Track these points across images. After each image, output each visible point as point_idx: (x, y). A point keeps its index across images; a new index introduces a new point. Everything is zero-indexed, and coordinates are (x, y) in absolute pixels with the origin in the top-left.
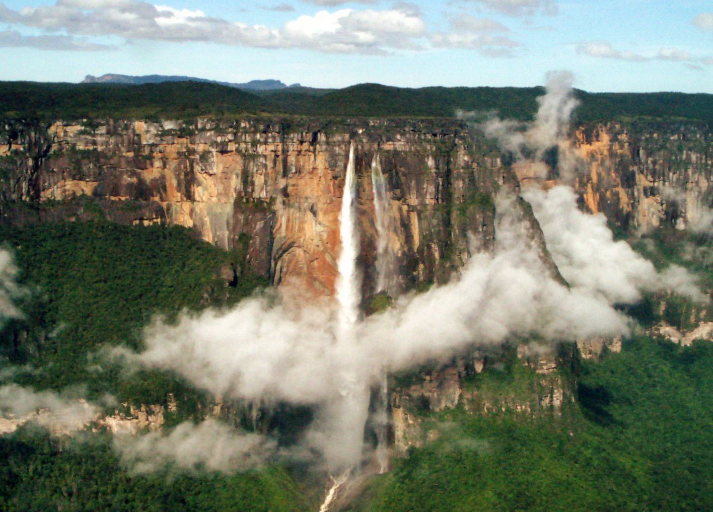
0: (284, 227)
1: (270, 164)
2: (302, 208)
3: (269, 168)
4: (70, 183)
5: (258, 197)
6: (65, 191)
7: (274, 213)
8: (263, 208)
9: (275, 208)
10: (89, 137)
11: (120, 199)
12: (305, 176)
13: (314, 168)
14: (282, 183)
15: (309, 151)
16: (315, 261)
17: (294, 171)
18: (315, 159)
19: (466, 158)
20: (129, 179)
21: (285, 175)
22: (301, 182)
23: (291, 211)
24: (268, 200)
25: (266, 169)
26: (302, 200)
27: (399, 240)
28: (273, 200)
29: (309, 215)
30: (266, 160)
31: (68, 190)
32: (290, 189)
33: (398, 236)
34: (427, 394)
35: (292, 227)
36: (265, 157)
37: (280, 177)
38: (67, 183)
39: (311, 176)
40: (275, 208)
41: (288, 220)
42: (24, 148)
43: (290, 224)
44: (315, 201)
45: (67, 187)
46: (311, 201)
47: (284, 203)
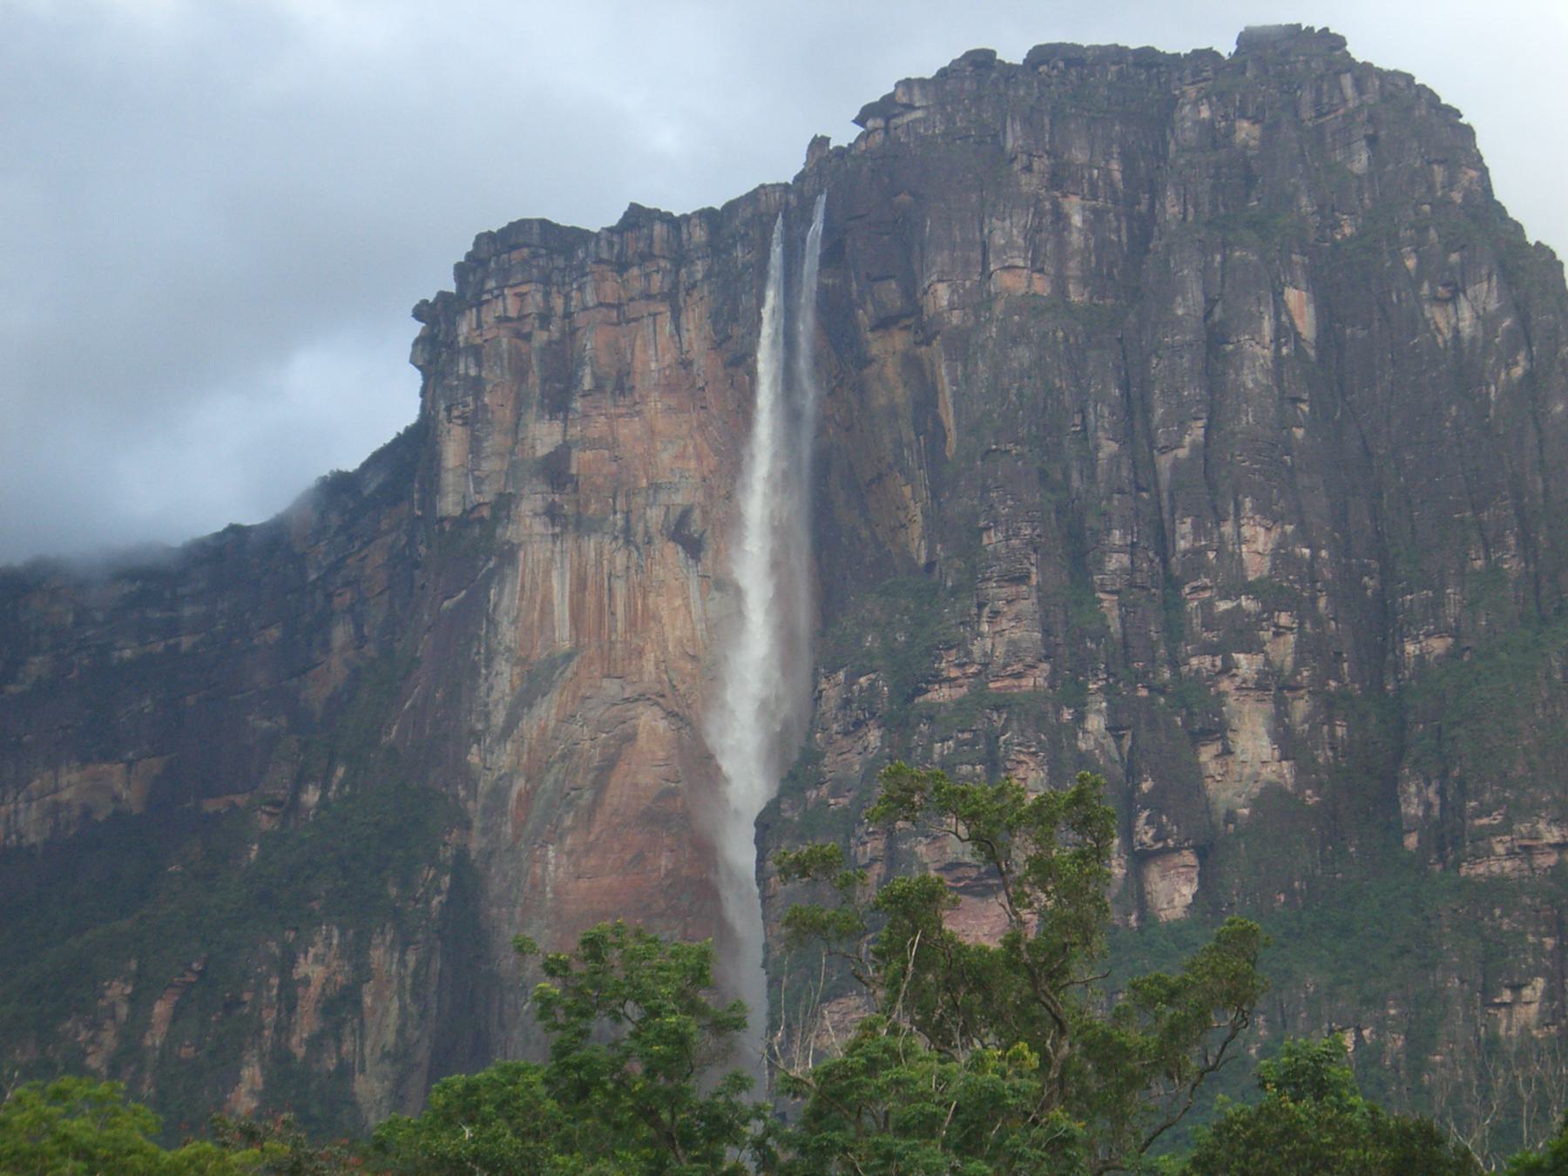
0: (561, 610)
1: (494, 374)
2: (640, 528)
3: (489, 388)
4: (75, 777)
5: (457, 512)
6: (57, 806)
7: (509, 555)
8: (476, 549)
9: (510, 533)
10: (156, 615)
11: (233, 806)
14: (544, 436)
15: (648, 296)
17: (587, 383)
18: (678, 328)
19: (1205, 113)
20: (266, 724)
21: (557, 405)
22: (629, 430)
23: (590, 545)
24: (486, 513)
25: (477, 398)
26: (640, 500)
28: (504, 505)
29: (673, 554)
30: (479, 365)
31: (68, 804)
32: (579, 461)
33: (910, 481)
36: (476, 351)
37: (530, 416)
38: (63, 781)
39: (673, 402)
40: (510, 533)
41: (580, 584)
43: (590, 600)
45: (66, 795)
46: (678, 499)
47: (552, 513)
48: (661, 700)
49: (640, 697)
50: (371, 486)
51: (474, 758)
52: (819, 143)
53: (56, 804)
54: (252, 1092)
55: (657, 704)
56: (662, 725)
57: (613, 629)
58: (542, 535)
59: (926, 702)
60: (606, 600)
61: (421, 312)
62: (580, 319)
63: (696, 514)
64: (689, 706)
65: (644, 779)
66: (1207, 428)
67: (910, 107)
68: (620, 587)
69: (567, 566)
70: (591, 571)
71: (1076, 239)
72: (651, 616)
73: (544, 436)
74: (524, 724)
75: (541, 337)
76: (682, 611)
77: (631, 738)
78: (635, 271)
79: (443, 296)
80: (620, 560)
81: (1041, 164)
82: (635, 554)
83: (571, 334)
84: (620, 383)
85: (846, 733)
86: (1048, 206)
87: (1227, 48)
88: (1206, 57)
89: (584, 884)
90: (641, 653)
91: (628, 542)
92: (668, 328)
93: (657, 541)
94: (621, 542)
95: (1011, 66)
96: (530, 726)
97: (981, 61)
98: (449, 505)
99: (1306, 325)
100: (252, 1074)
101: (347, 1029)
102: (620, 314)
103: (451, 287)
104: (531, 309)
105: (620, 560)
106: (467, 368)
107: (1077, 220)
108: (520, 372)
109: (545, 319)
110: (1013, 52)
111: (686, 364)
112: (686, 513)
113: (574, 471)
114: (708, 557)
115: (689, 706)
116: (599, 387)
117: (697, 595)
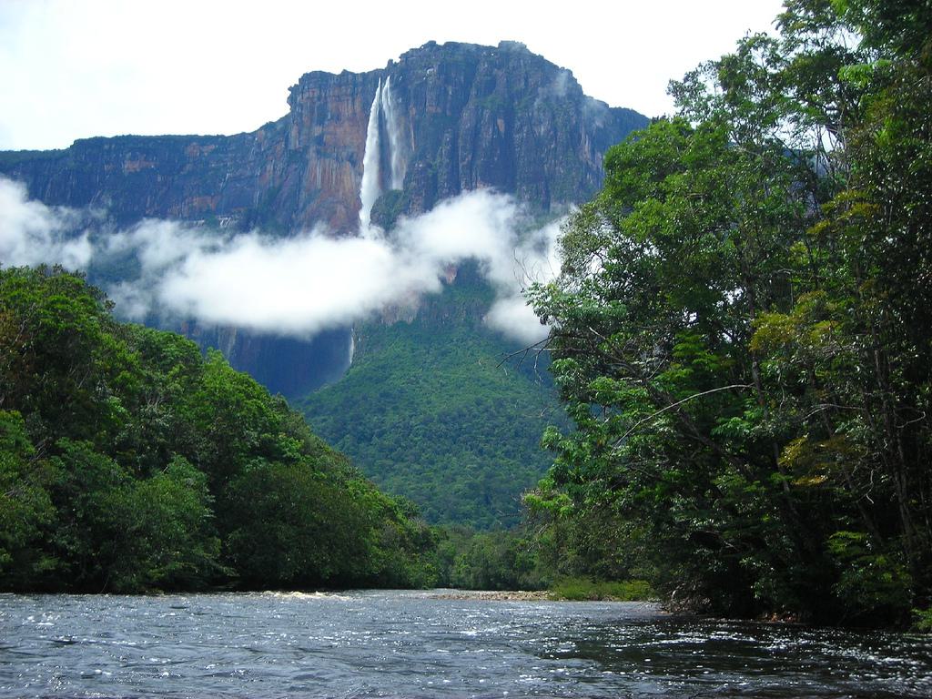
7: (306, 163)
9: (307, 157)
12: (344, 122)
13: (354, 114)
14: (317, 131)
15: (346, 95)
17: (329, 117)
21: (321, 123)
23: (327, 161)
26: (340, 150)
28: (306, 149)
29: (348, 164)
31: (195, 207)
36: (301, 106)
40: (307, 157)
41: (324, 171)
42: (155, 165)
44: (356, 150)
46: (350, 150)
47: (318, 152)
49: (337, 202)
50: (279, 127)
51: (294, 216)
52: (390, 61)
53: (193, 206)
59: (240, 370)
61: (289, 89)
62: (328, 100)
63: (355, 155)
66: (472, 157)
67: (412, 56)
68: (334, 173)
71: (449, 98)
72: (342, 181)
73: (317, 131)
74: (307, 207)
75: (318, 103)
77: (335, 212)
78: (343, 87)
79: (295, 85)
81: (442, 77)
83: (326, 103)
84: (337, 118)
86: (443, 89)
87: (497, 46)
88: (491, 48)
90: (338, 191)
91: (337, 159)
92: (350, 102)
95: (440, 46)
96: (309, 209)
97: (432, 44)
98: (292, 147)
99: (502, 129)
102: (339, 98)
103: (298, 83)
104: (316, 95)
105: (335, 166)
107: (450, 93)
108: (312, 112)
109: (319, 99)
110: (441, 42)
111: (354, 114)
112: (353, 154)
114: (357, 168)
116: (332, 118)
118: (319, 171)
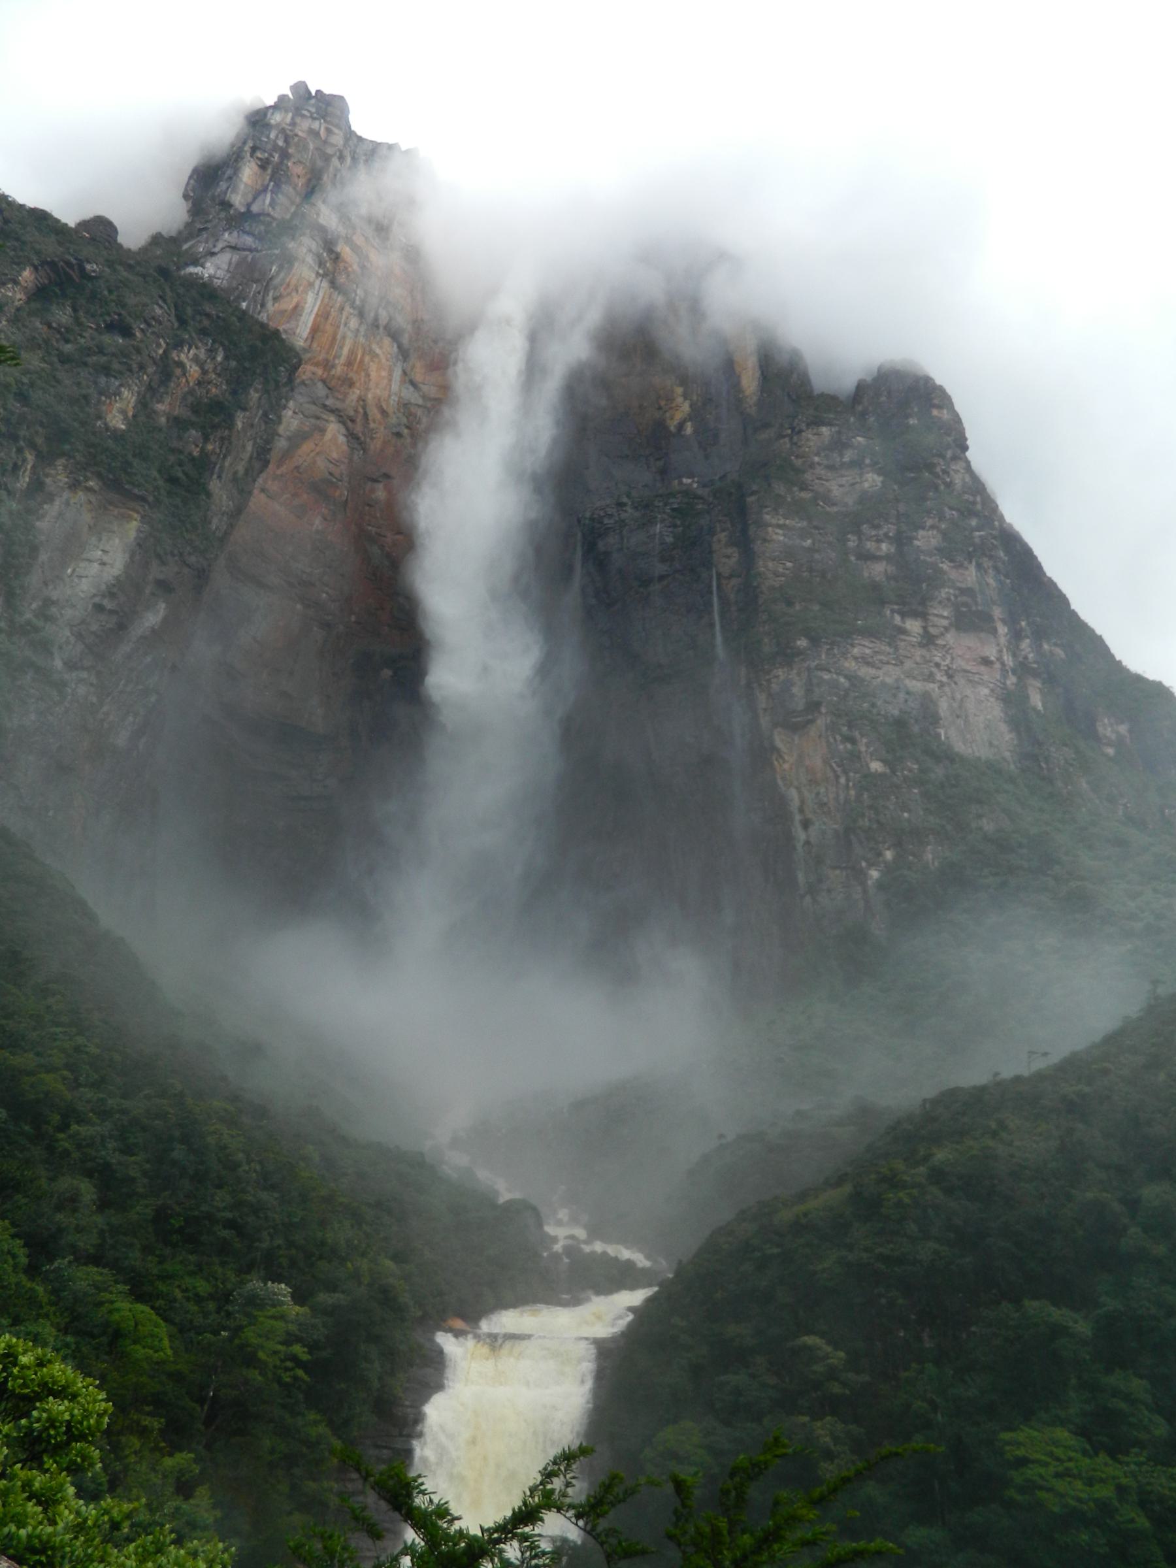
5: (243, 210)
16: (381, 486)
23: (340, 299)
27: (685, 396)
34: (916, 686)
35: (334, 338)
48: (349, 423)
54: (123, 412)
55: (344, 423)
56: (342, 439)
57: (336, 357)
58: (311, 267)
60: (339, 337)
64: (372, 438)
65: (321, 464)
69: (321, 294)
70: (333, 313)
76: (385, 381)
80: (354, 323)
82: (363, 329)
85: (831, 468)
89: (262, 496)
90: (351, 384)
93: (381, 329)
94: (356, 312)
100: (128, 398)
101: (219, 434)
106: (277, 137)
113: (338, 249)
115: (372, 438)
117: (398, 379)
118: (312, 304)
